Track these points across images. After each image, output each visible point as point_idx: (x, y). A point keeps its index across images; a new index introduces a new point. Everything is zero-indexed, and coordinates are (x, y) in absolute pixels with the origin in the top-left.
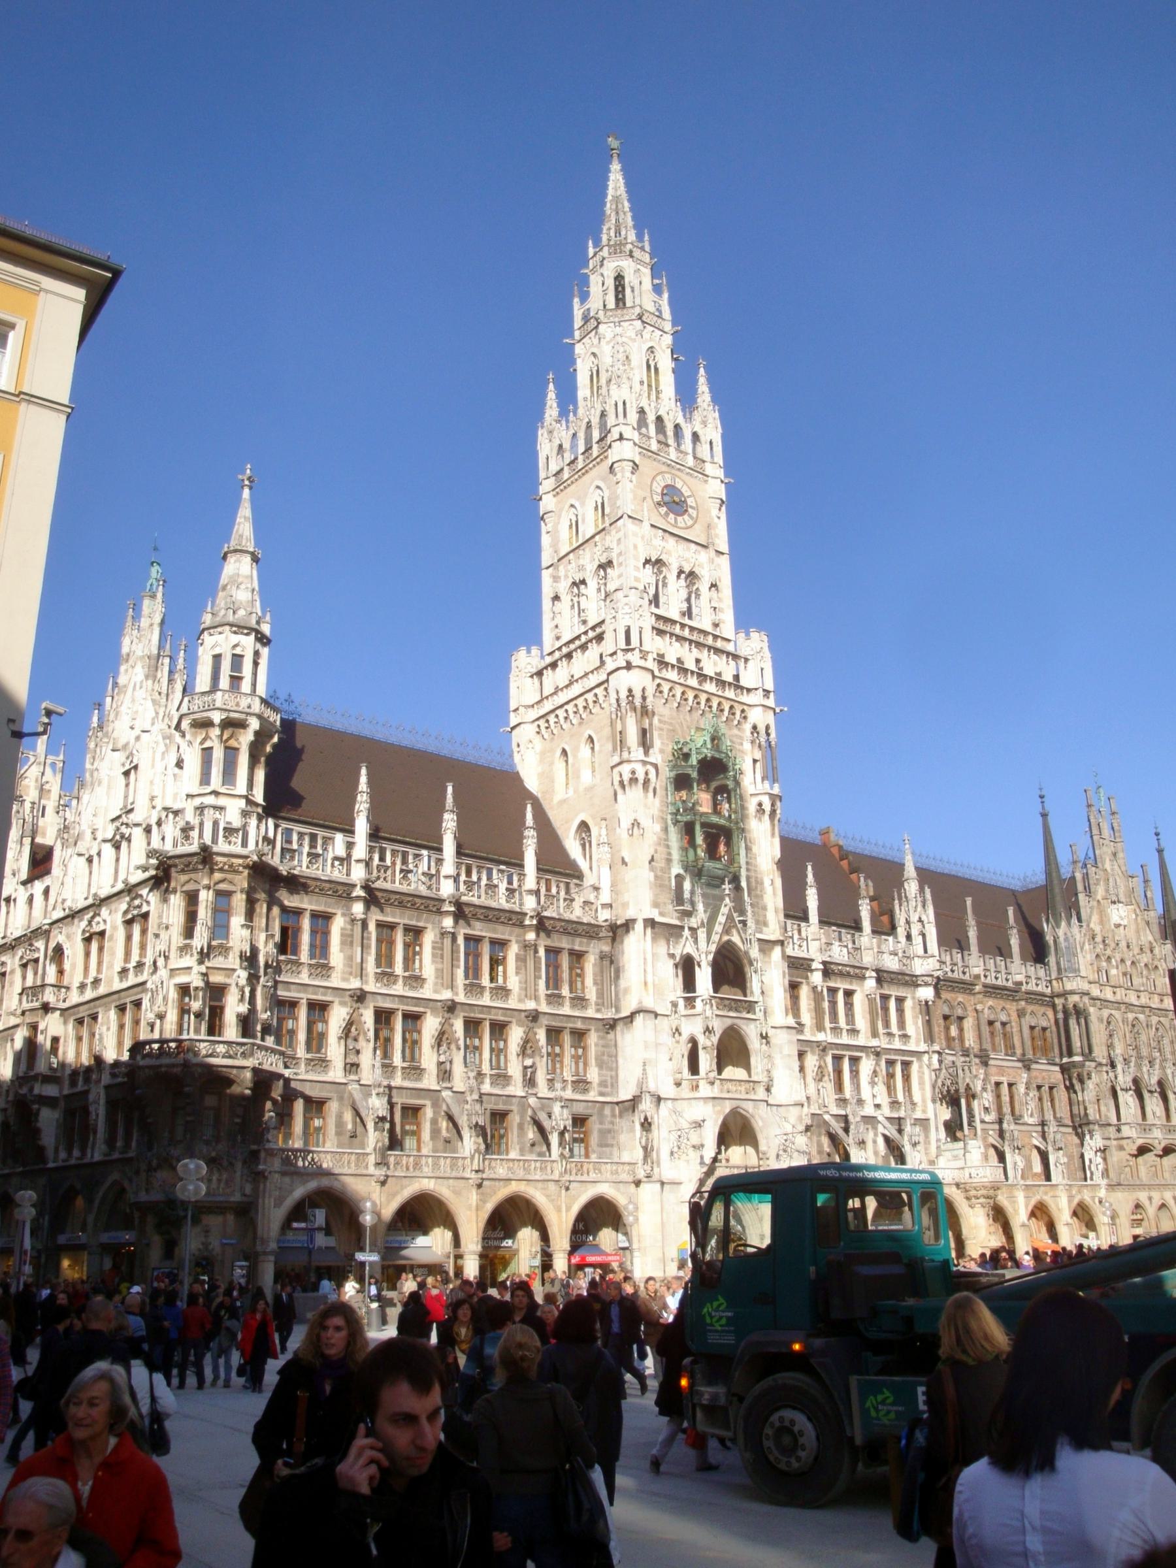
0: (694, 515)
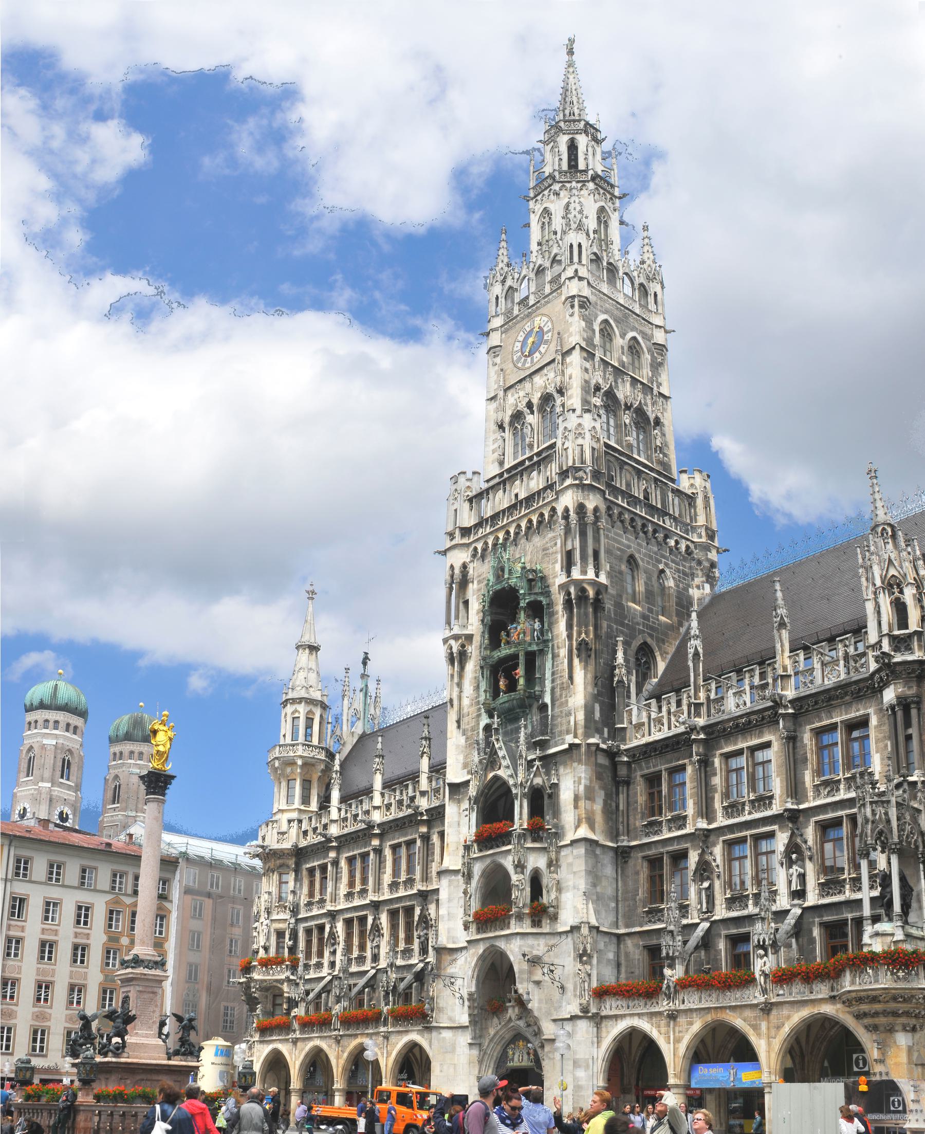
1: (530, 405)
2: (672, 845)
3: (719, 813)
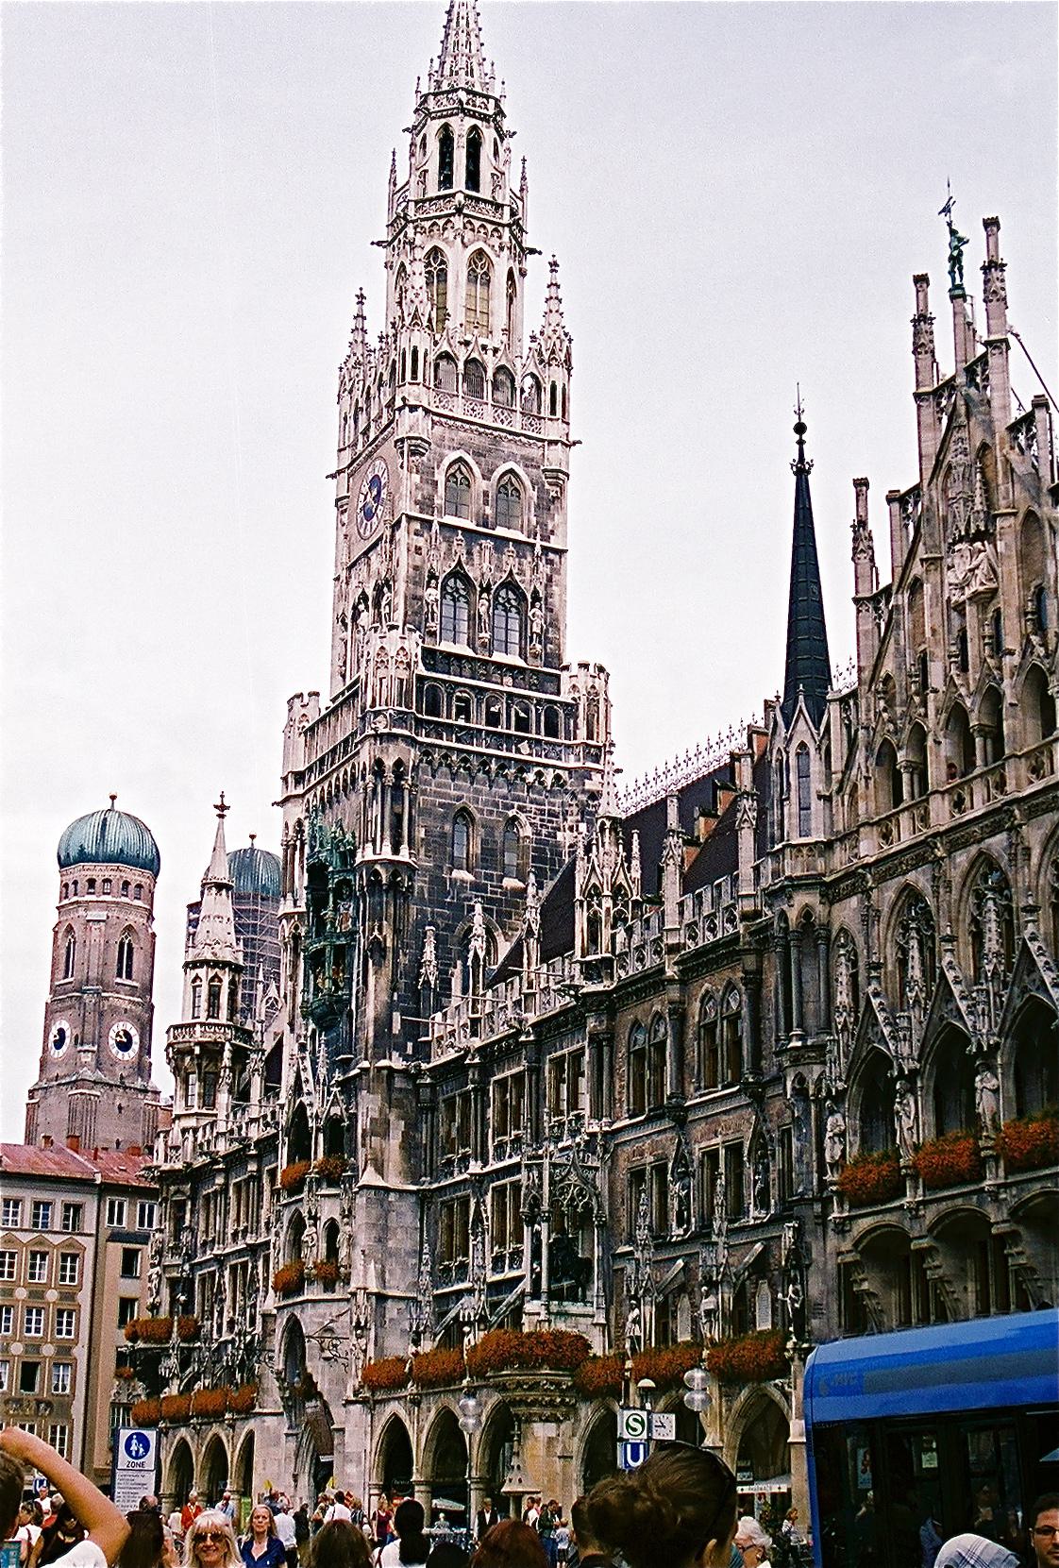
1: (364, 597)
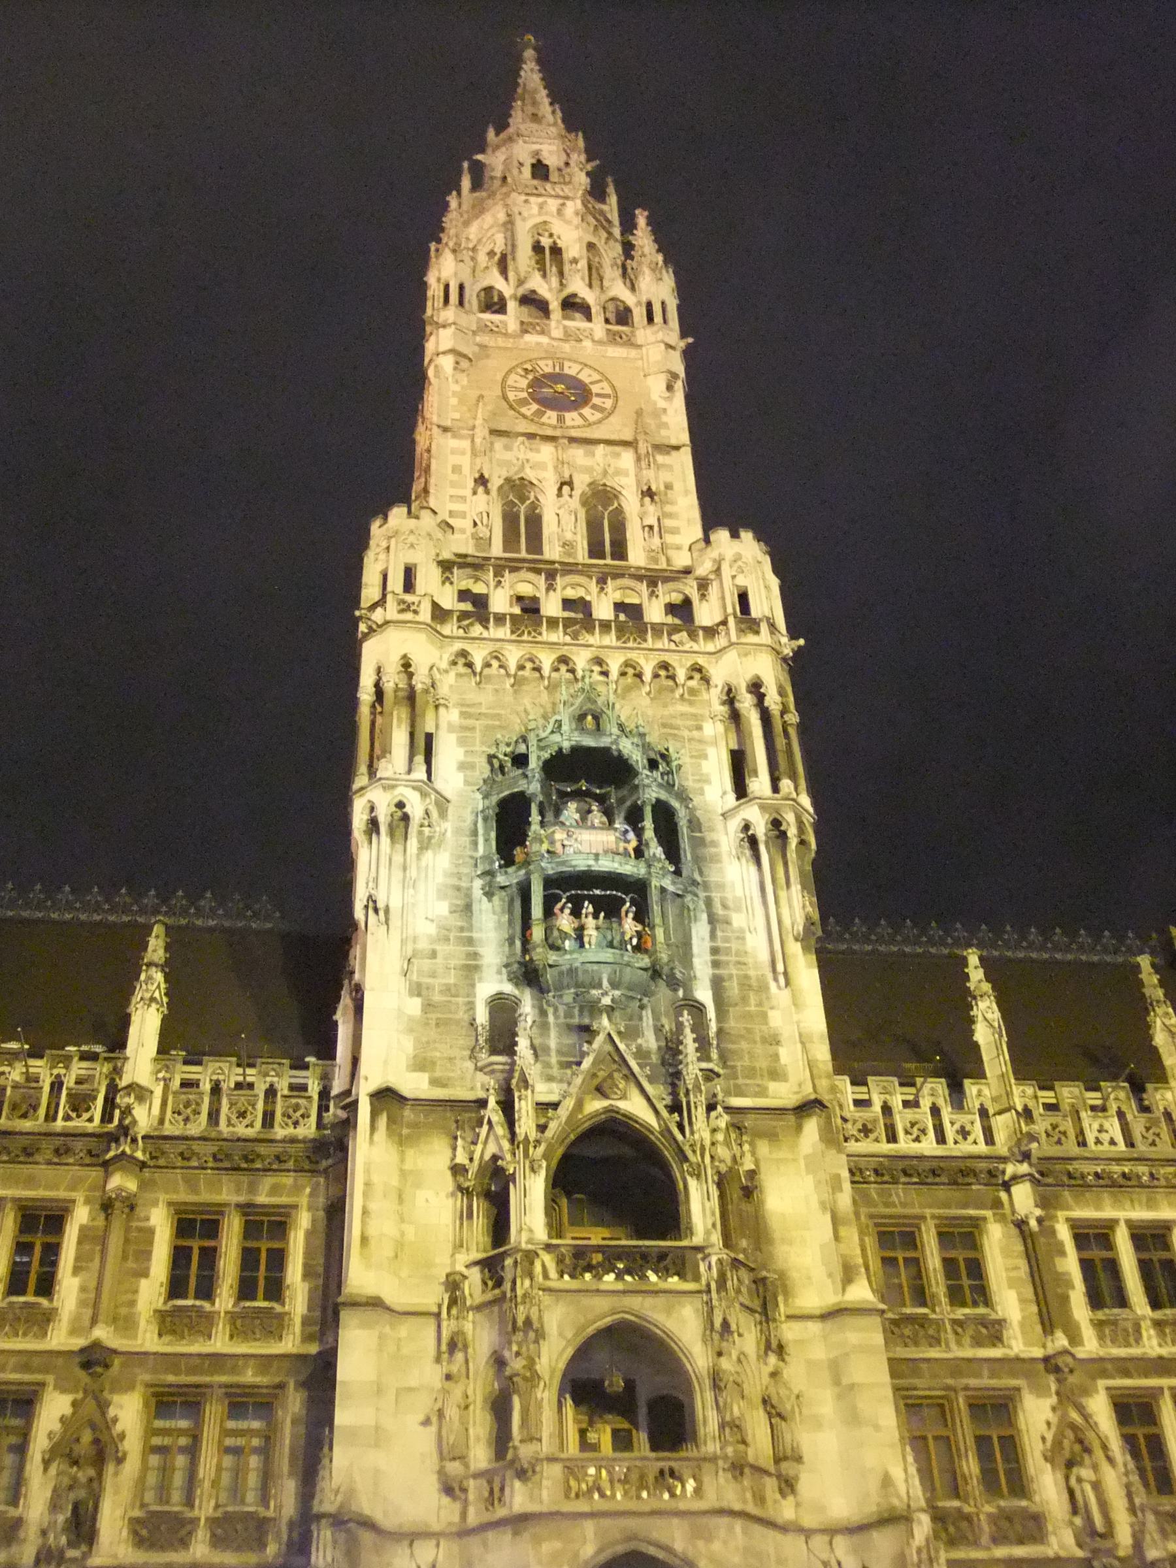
0: (608, 404)
2: (978, 1375)
3: (1088, 1334)
